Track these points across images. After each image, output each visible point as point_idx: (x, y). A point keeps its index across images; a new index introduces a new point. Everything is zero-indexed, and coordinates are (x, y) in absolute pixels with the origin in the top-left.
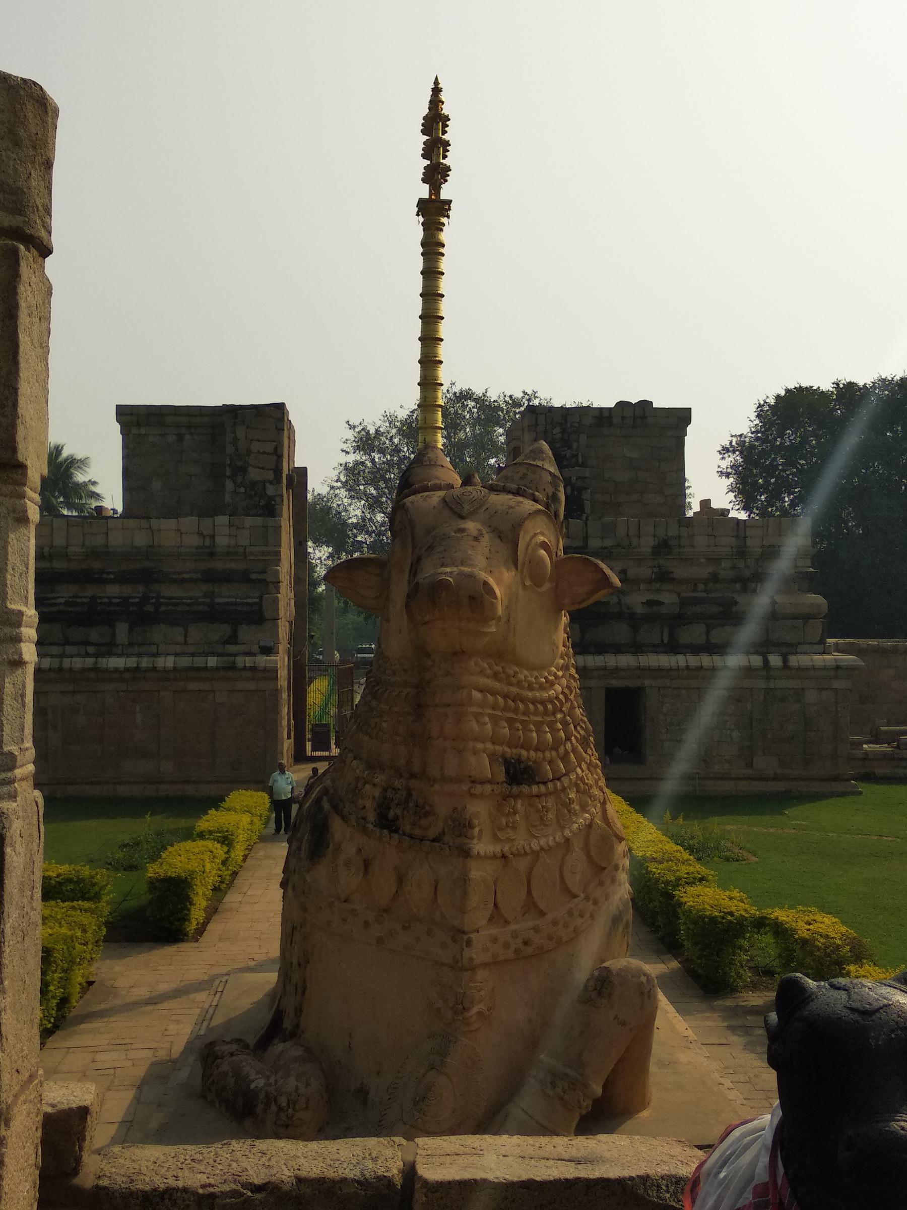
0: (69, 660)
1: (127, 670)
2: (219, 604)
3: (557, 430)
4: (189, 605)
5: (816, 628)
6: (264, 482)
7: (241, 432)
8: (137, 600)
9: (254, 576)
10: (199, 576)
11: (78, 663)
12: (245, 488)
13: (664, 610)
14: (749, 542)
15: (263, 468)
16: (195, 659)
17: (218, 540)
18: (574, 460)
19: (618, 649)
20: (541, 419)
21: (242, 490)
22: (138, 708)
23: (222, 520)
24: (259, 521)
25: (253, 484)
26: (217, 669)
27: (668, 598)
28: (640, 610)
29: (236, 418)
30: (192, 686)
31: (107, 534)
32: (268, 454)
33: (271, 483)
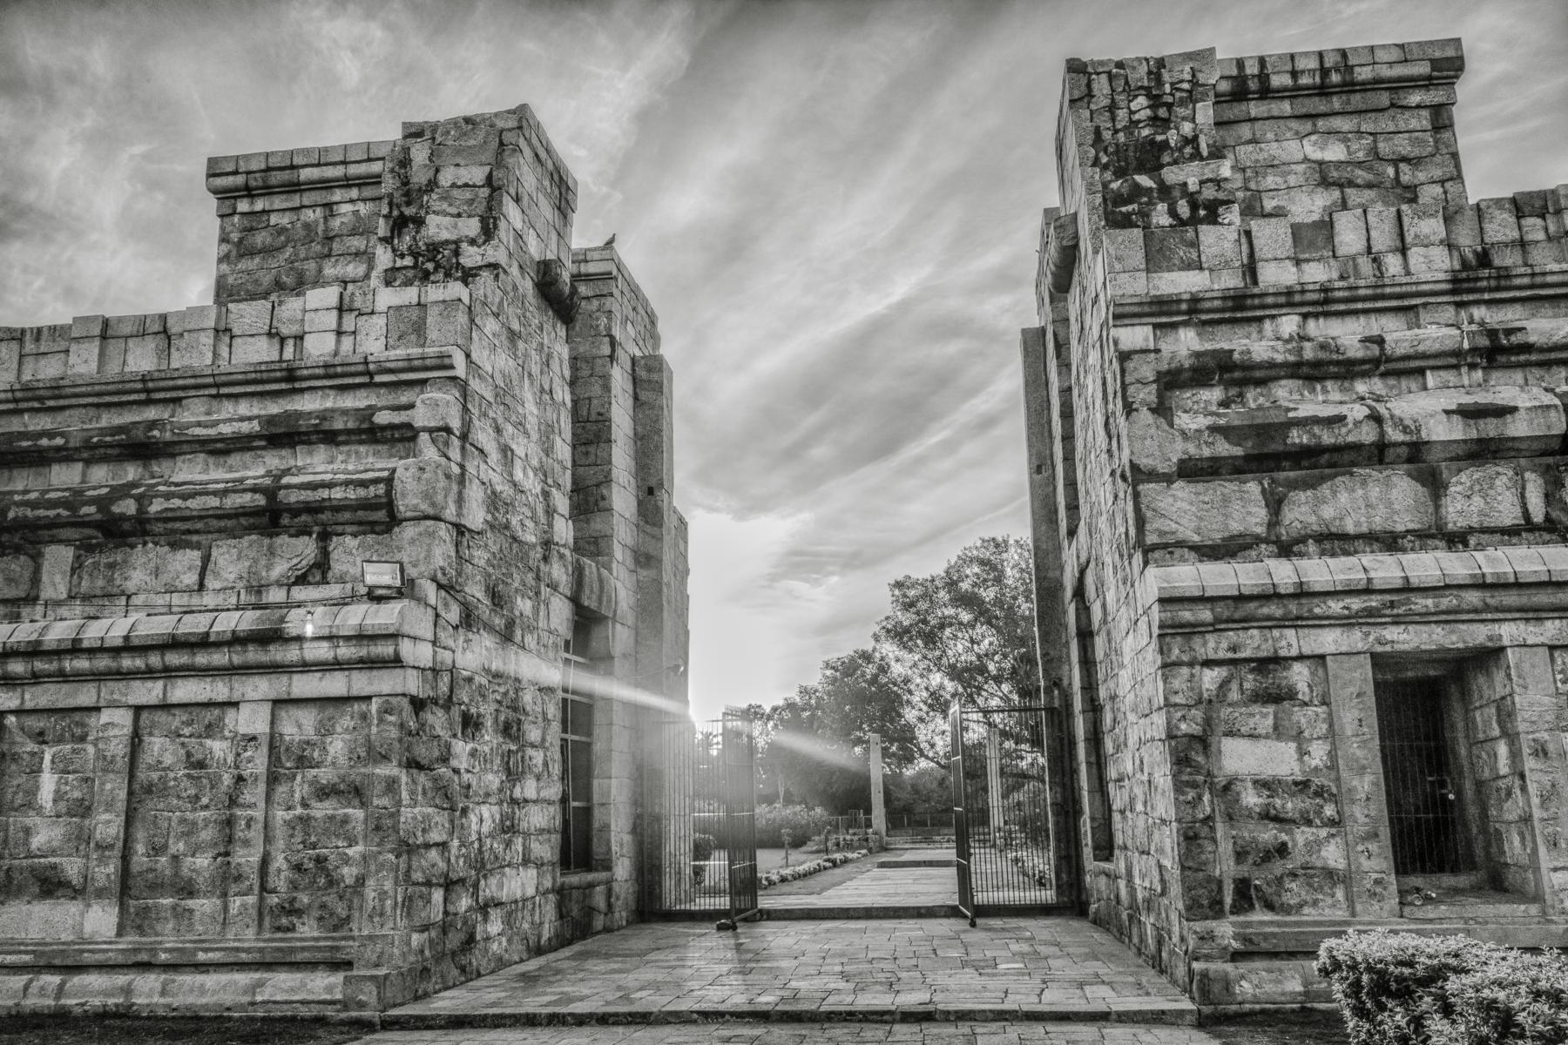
2: (288, 487)
4: (215, 493)
6: (457, 242)
8: (104, 491)
10: (255, 426)
13: (1518, 427)
15: (459, 215)
21: (408, 261)
22: (47, 758)
25: (434, 248)
26: (237, 640)
30: (185, 691)
32: (474, 186)
33: (473, 242)
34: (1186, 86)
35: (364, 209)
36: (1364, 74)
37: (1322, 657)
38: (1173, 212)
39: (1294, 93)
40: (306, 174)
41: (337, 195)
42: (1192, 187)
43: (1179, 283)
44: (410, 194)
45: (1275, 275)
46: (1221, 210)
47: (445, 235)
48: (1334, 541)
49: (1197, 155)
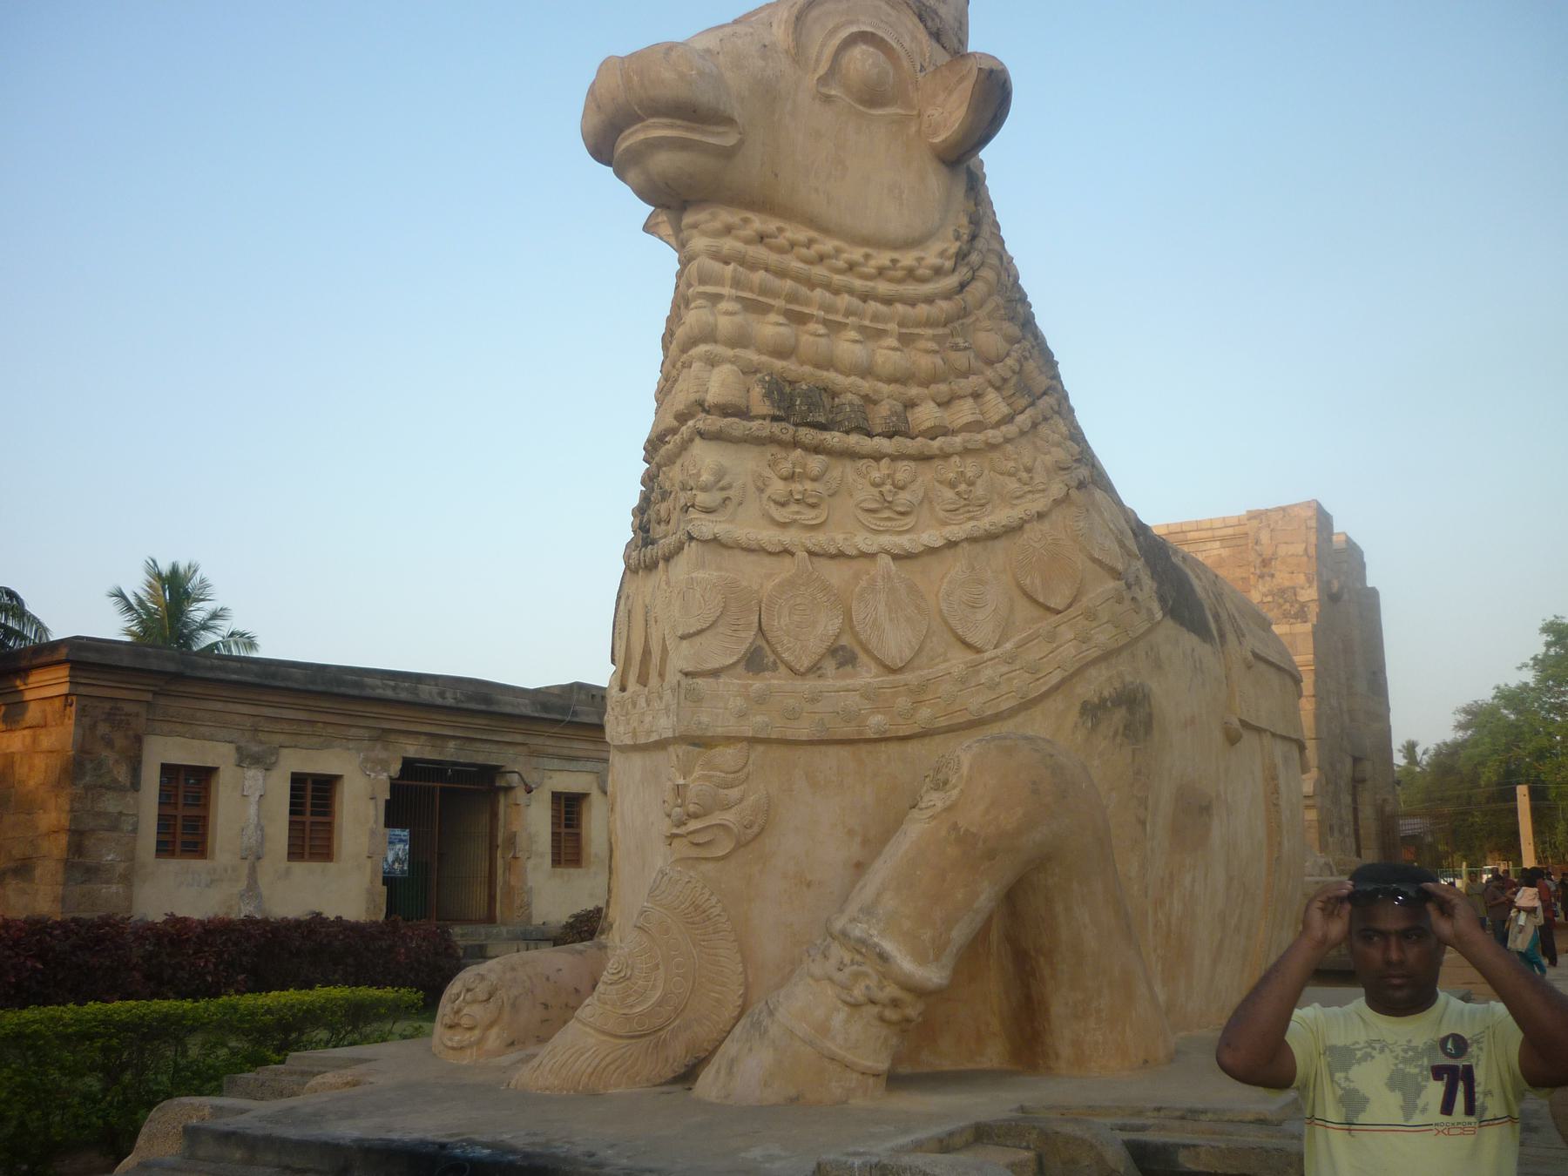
7: (1265, 537)
12: (1273, 595)
21: (1269, 599)
25: (1282, 591)
33: (1303, 588)
35: (1225, 552)
40: (1191, 535)
41: (1209, 545)
44: (1265, 563)
47: (1287, 584)
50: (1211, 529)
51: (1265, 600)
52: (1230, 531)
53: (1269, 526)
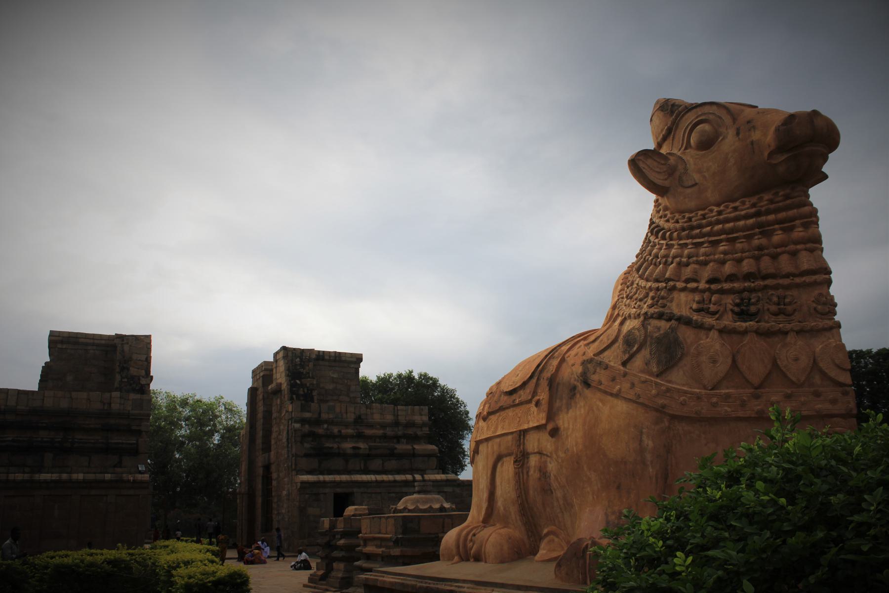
0: (13, 475)
1: (52, 481)
3: (298, 359)
5: (434, 462)
7: (126, 348)
8: (60, 440)
9: (134, 428)
11: (19, 477)
13: (361, 452)
14: (400, 418)
15: (138, 369)
16: (97, 475)
17: (113, 405)
18: (307, 375)
19: (339, 472)
20: (290, 354)
21: (126, 380)
23: (116, 394)
24: (138, 396)
27: (362, 445)
28: (349, 451)
29: (123, 340)
31: (43, 400)
32: (142, 361)
33: (143, 377)
34: (308, 358)
36: (343, 359)
37: (325, 494)
38: (304, 391)
39: (329, 360)
41: (89, 348)
42: (308, 385)
43: (307, 415)
45: (324, 416)
46: (313, 392)
48: (330, 472)
49: (309, 377)
50: (93, 339)
51: (123, 380)
52: (103, 342)
53: (128, 343)
